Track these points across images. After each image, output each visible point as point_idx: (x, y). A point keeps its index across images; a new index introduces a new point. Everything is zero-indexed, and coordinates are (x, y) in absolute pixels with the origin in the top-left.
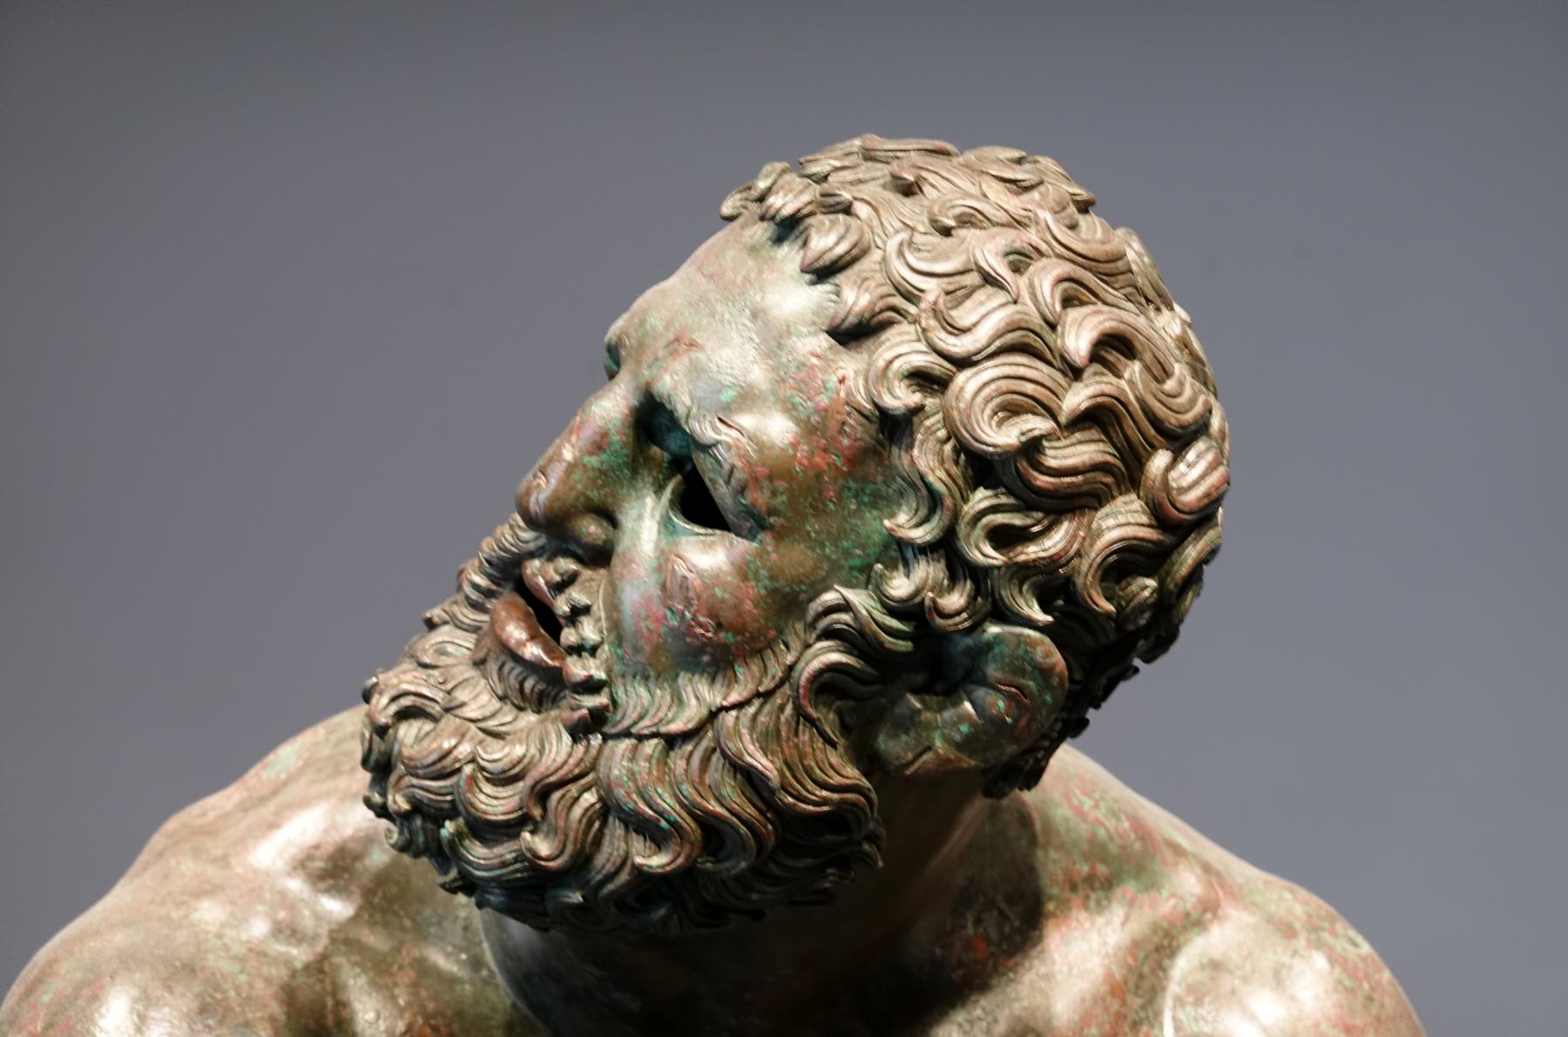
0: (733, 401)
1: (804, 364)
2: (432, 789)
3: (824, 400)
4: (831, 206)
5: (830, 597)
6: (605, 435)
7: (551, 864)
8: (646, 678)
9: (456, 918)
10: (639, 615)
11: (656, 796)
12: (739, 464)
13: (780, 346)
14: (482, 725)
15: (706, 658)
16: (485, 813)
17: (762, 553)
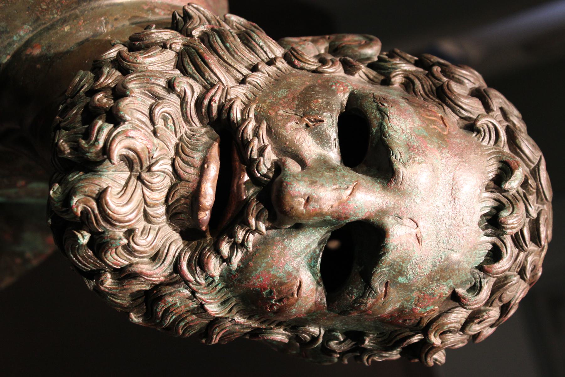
0: (400, 284)
1: (433, 296)
2: (98, 222)
3: (419, 309)
4: (519, 243)
5: (314, 330)
6: (346, 218)
7: (102, 288)
8: (227, 287)
9: (12, 37)
10: (259, 278)
11: (170, 317)
12: (368, 306)
13: (438, 280)
14: (147, 209)
15: (254, 308)
16: (106, 258)
17: (325, 314)
